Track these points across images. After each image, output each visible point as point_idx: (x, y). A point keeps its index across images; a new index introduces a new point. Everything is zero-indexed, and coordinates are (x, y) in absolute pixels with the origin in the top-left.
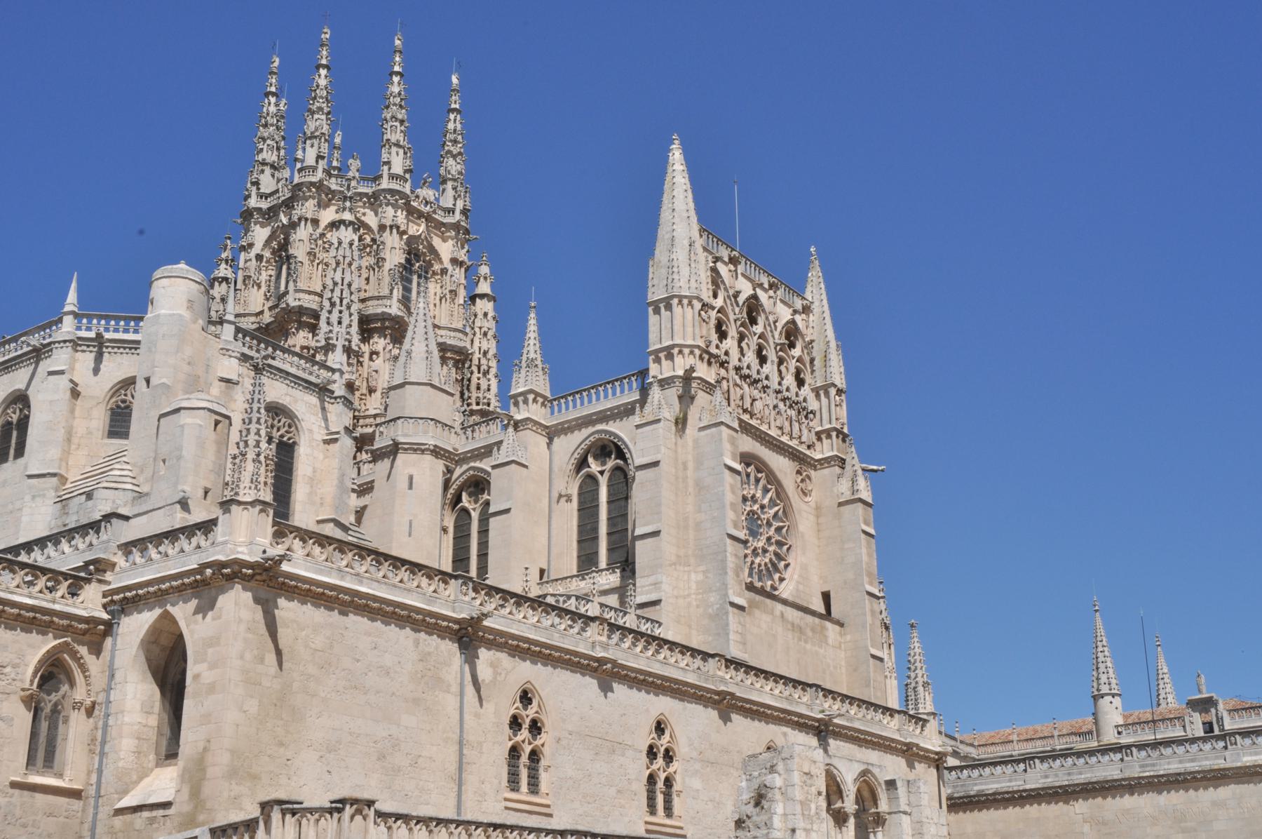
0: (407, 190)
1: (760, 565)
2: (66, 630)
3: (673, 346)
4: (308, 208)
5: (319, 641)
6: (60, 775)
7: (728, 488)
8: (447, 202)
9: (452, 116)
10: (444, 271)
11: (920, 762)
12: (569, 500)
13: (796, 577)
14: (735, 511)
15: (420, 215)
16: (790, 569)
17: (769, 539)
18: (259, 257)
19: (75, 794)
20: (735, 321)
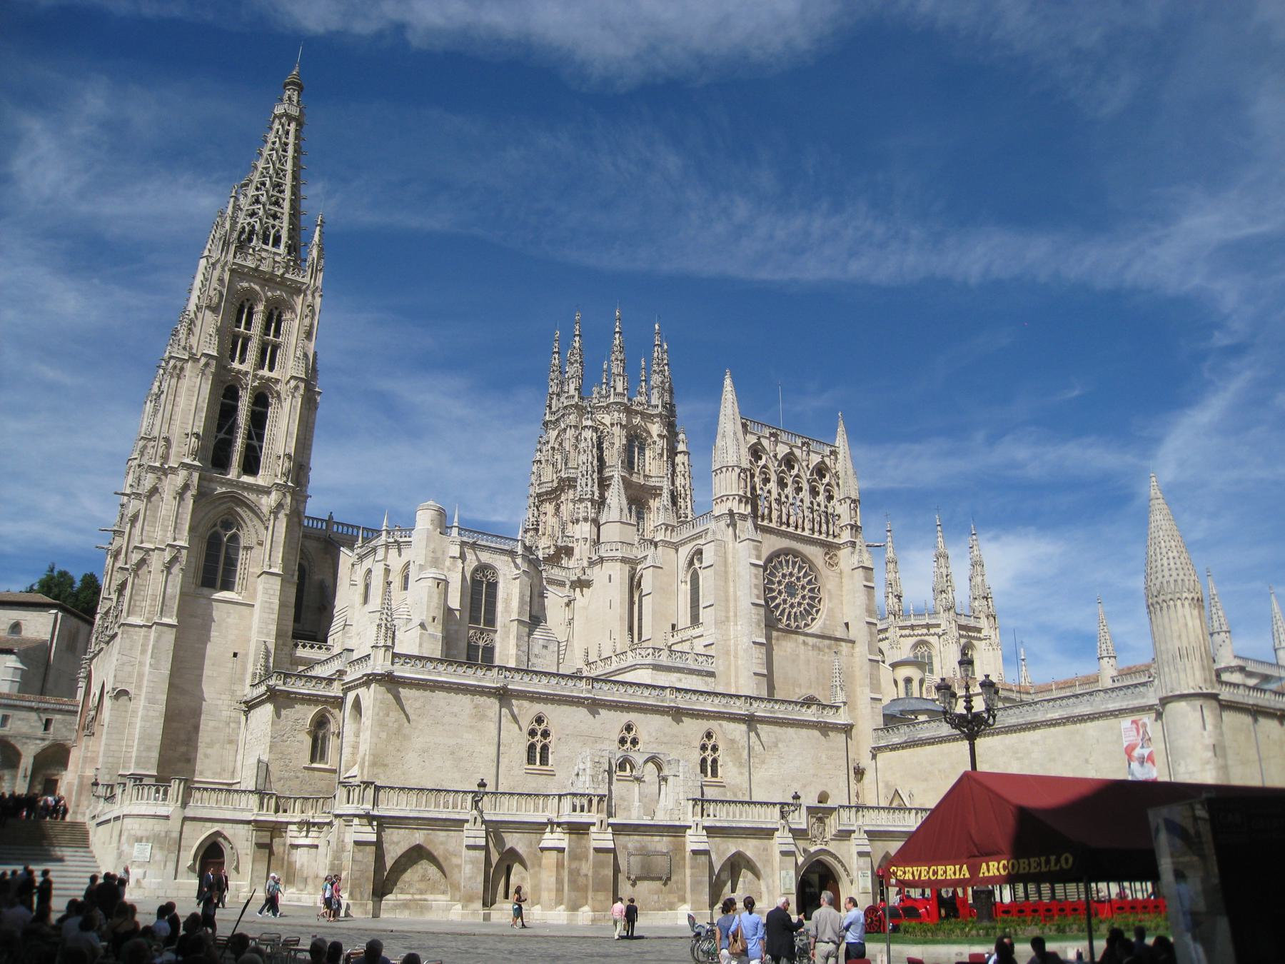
0: (626, 401)
1: (795, 613)
2: (326, 702)
3: (723, 496)
4: (572, 419)
5: (417, 705)
6: (327, 763)
7: (753, 575)
8: (654, 402)
9: (656, 349)
10: (654, 443)
11: (832, 731)
12: (686, 582)
13: (824, 616)
14: (758, 589)
15: (637, 412)
16: (820, 612)
17: (803, 597)
18: (553, 448)
19: (334, 771)
20: (775, 471)
